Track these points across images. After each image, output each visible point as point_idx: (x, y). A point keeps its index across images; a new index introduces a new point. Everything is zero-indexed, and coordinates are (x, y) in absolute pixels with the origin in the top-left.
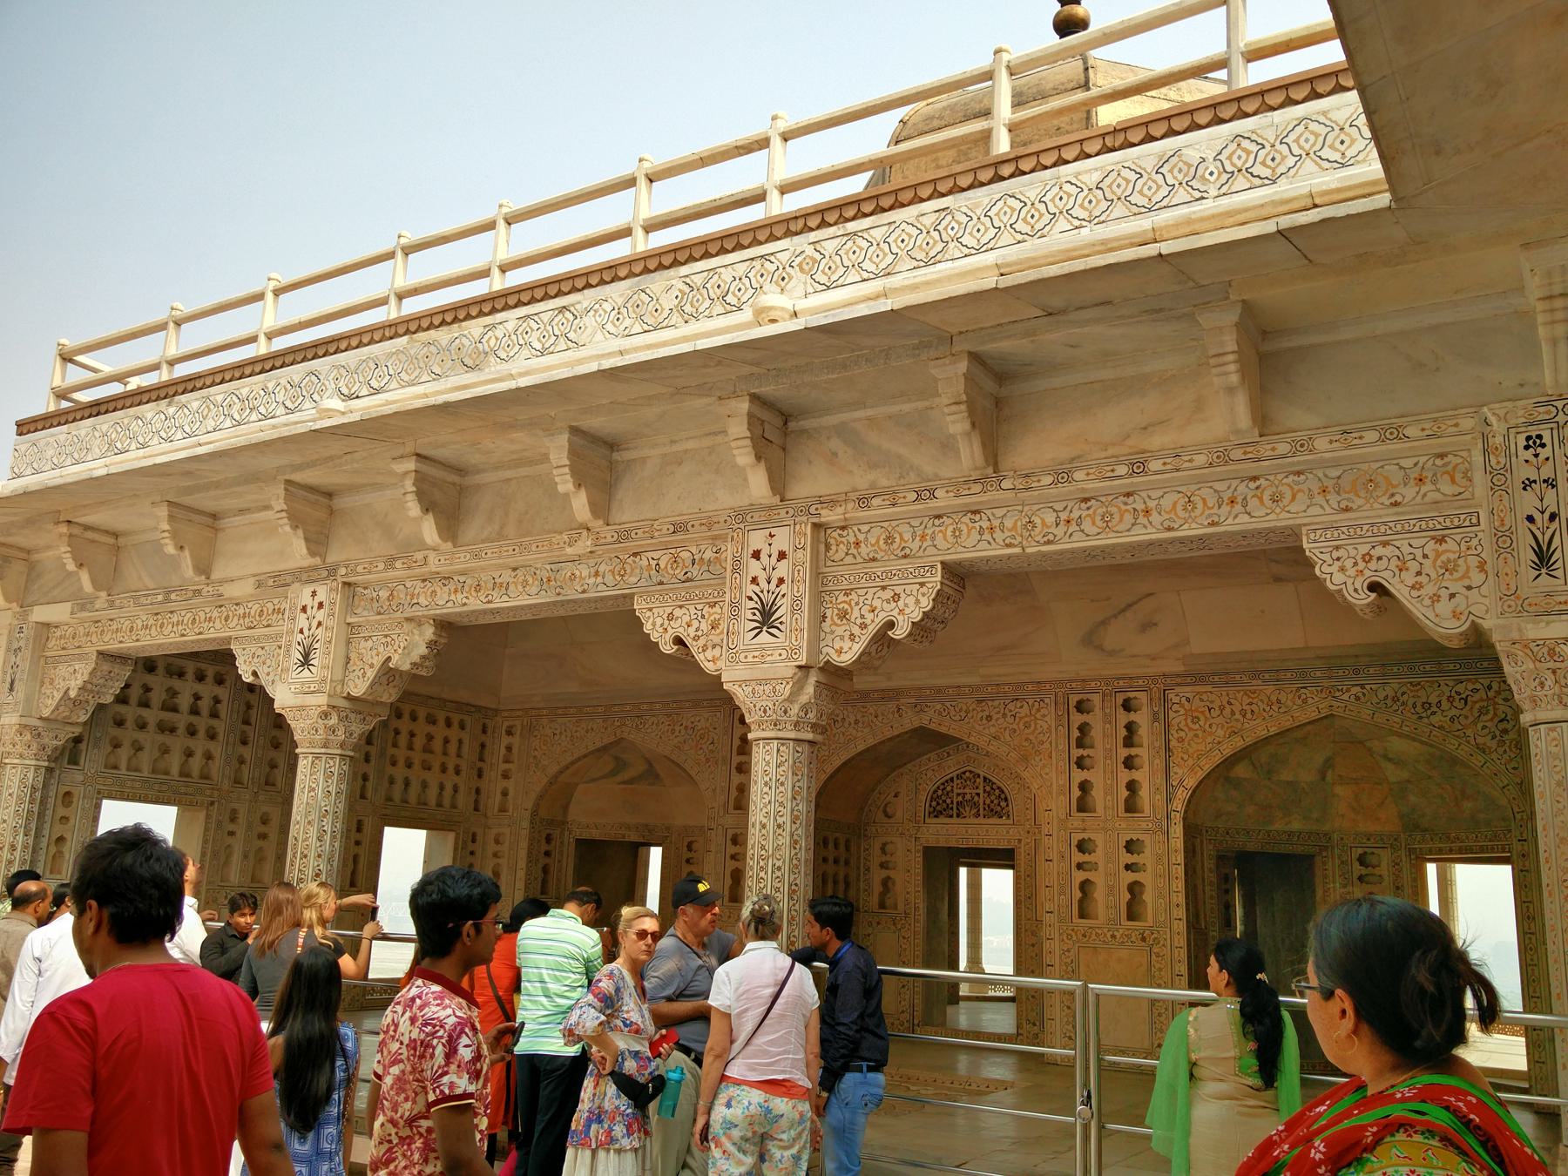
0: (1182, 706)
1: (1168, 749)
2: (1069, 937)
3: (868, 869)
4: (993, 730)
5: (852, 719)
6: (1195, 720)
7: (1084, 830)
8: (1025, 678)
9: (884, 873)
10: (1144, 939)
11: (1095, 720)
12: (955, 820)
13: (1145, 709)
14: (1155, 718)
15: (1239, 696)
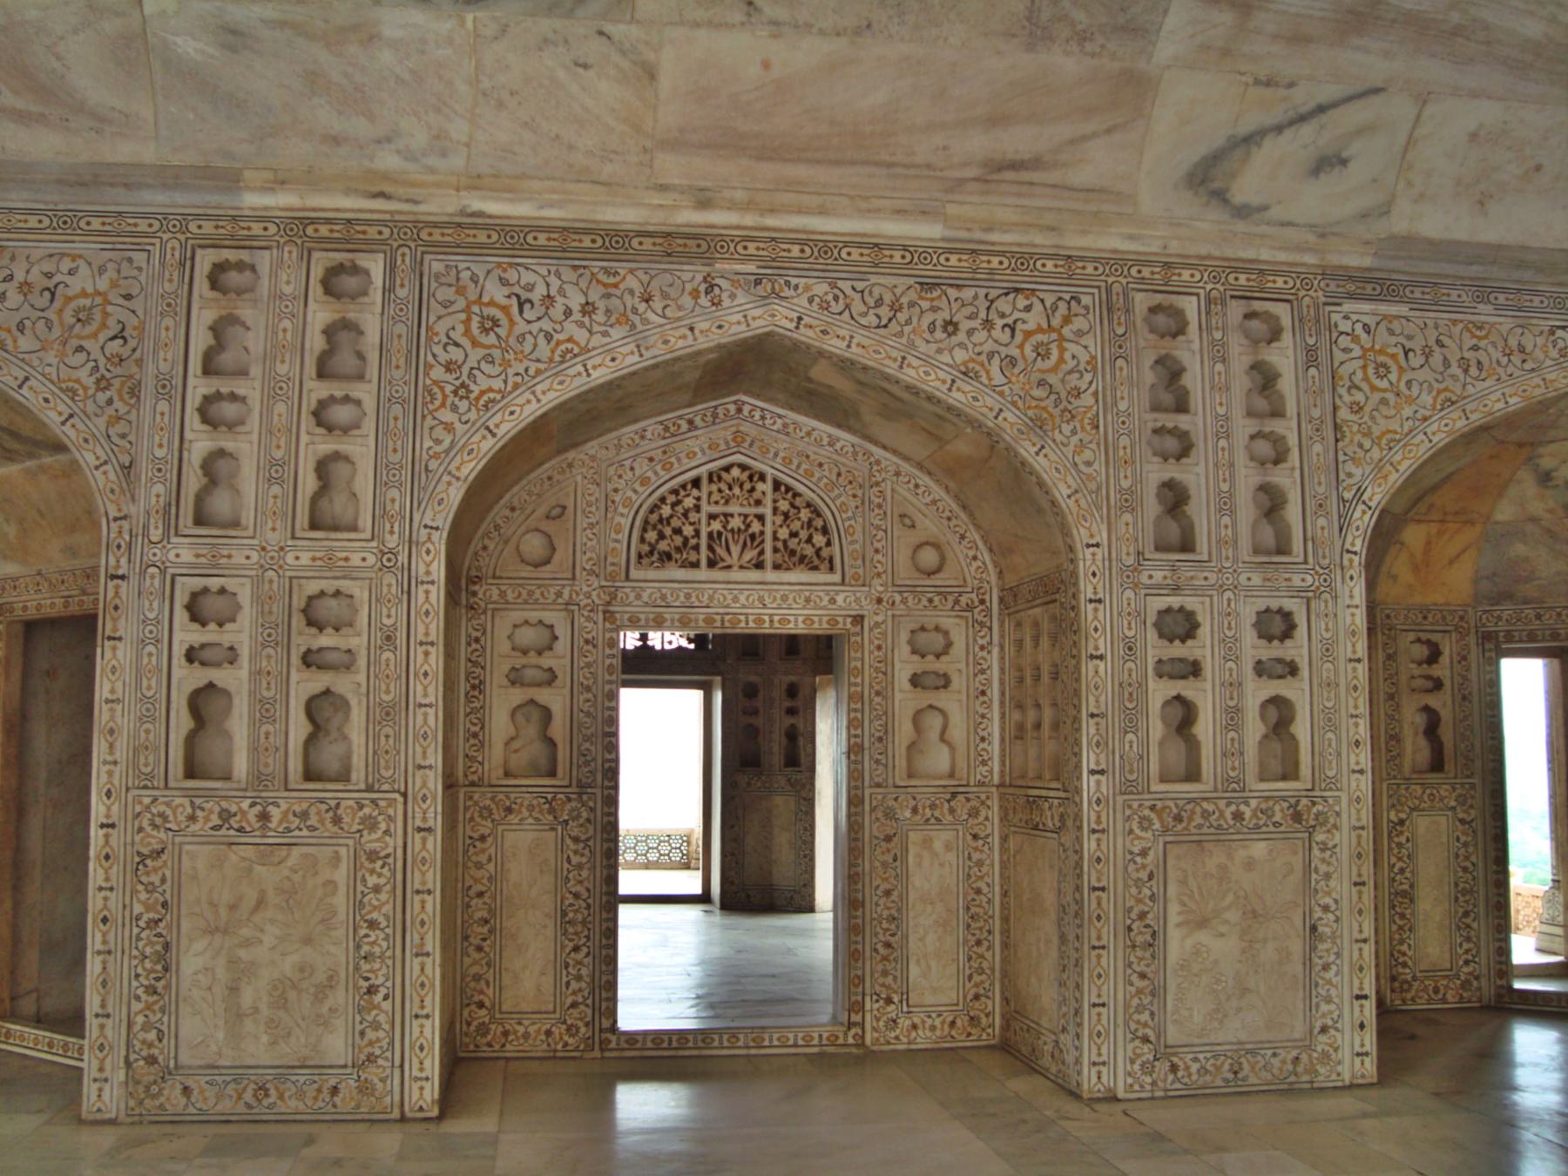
0: (1356, 339)
1: (1336, 427)
2: (1145, 824)
3: (478, 687)
4: (960, 356)
5: (576, 300)
6: (1382, 370)
7: (1176, 589)
8: (1041, 240)
9: (518, 696)
10: (1297, 817)
11: (1190, 352)
12: (703, 573)
13: (1287, 337)
14: (1311, 357)
15: (1457, 329)
